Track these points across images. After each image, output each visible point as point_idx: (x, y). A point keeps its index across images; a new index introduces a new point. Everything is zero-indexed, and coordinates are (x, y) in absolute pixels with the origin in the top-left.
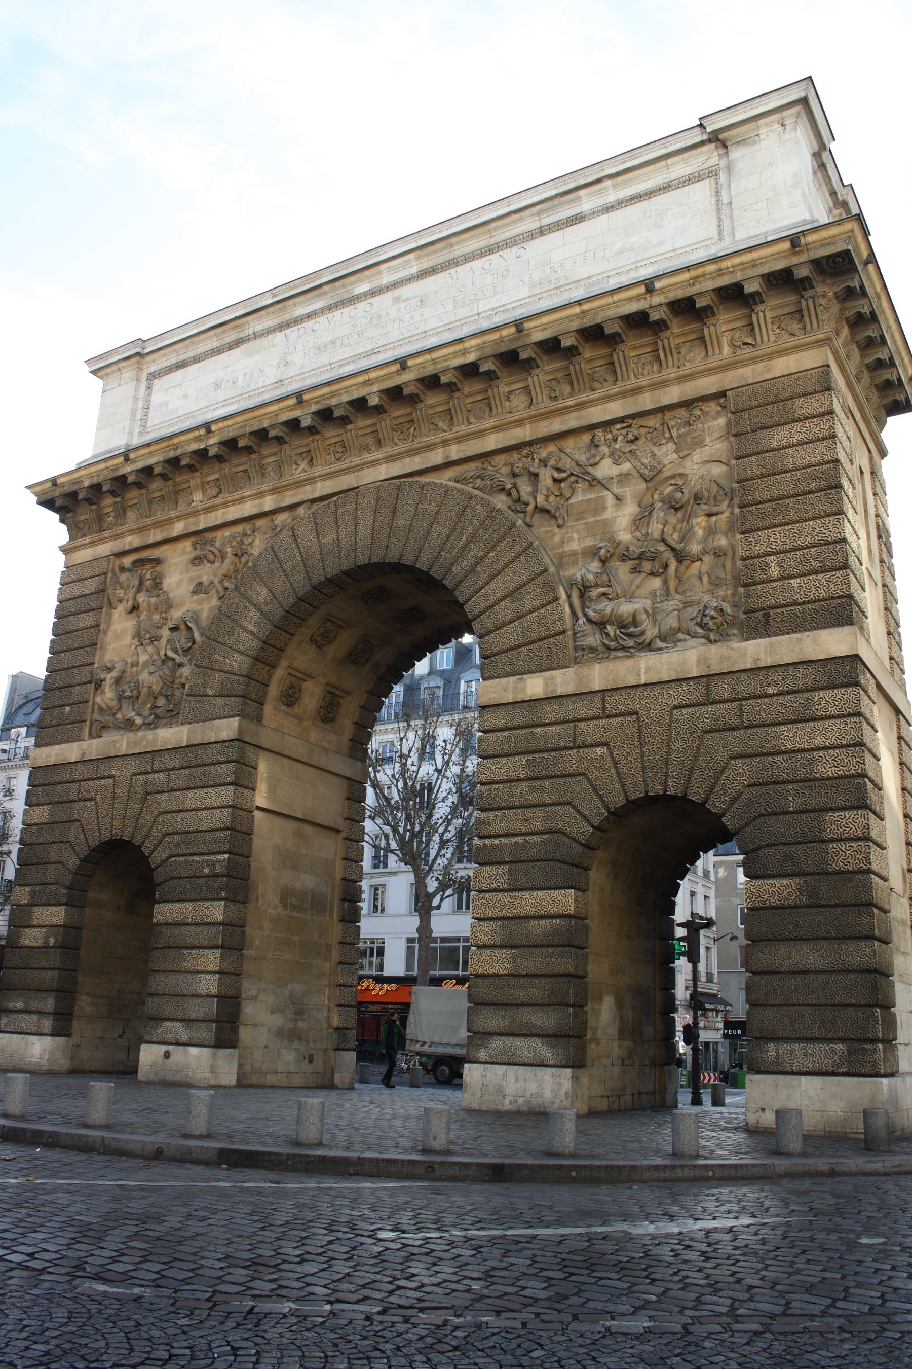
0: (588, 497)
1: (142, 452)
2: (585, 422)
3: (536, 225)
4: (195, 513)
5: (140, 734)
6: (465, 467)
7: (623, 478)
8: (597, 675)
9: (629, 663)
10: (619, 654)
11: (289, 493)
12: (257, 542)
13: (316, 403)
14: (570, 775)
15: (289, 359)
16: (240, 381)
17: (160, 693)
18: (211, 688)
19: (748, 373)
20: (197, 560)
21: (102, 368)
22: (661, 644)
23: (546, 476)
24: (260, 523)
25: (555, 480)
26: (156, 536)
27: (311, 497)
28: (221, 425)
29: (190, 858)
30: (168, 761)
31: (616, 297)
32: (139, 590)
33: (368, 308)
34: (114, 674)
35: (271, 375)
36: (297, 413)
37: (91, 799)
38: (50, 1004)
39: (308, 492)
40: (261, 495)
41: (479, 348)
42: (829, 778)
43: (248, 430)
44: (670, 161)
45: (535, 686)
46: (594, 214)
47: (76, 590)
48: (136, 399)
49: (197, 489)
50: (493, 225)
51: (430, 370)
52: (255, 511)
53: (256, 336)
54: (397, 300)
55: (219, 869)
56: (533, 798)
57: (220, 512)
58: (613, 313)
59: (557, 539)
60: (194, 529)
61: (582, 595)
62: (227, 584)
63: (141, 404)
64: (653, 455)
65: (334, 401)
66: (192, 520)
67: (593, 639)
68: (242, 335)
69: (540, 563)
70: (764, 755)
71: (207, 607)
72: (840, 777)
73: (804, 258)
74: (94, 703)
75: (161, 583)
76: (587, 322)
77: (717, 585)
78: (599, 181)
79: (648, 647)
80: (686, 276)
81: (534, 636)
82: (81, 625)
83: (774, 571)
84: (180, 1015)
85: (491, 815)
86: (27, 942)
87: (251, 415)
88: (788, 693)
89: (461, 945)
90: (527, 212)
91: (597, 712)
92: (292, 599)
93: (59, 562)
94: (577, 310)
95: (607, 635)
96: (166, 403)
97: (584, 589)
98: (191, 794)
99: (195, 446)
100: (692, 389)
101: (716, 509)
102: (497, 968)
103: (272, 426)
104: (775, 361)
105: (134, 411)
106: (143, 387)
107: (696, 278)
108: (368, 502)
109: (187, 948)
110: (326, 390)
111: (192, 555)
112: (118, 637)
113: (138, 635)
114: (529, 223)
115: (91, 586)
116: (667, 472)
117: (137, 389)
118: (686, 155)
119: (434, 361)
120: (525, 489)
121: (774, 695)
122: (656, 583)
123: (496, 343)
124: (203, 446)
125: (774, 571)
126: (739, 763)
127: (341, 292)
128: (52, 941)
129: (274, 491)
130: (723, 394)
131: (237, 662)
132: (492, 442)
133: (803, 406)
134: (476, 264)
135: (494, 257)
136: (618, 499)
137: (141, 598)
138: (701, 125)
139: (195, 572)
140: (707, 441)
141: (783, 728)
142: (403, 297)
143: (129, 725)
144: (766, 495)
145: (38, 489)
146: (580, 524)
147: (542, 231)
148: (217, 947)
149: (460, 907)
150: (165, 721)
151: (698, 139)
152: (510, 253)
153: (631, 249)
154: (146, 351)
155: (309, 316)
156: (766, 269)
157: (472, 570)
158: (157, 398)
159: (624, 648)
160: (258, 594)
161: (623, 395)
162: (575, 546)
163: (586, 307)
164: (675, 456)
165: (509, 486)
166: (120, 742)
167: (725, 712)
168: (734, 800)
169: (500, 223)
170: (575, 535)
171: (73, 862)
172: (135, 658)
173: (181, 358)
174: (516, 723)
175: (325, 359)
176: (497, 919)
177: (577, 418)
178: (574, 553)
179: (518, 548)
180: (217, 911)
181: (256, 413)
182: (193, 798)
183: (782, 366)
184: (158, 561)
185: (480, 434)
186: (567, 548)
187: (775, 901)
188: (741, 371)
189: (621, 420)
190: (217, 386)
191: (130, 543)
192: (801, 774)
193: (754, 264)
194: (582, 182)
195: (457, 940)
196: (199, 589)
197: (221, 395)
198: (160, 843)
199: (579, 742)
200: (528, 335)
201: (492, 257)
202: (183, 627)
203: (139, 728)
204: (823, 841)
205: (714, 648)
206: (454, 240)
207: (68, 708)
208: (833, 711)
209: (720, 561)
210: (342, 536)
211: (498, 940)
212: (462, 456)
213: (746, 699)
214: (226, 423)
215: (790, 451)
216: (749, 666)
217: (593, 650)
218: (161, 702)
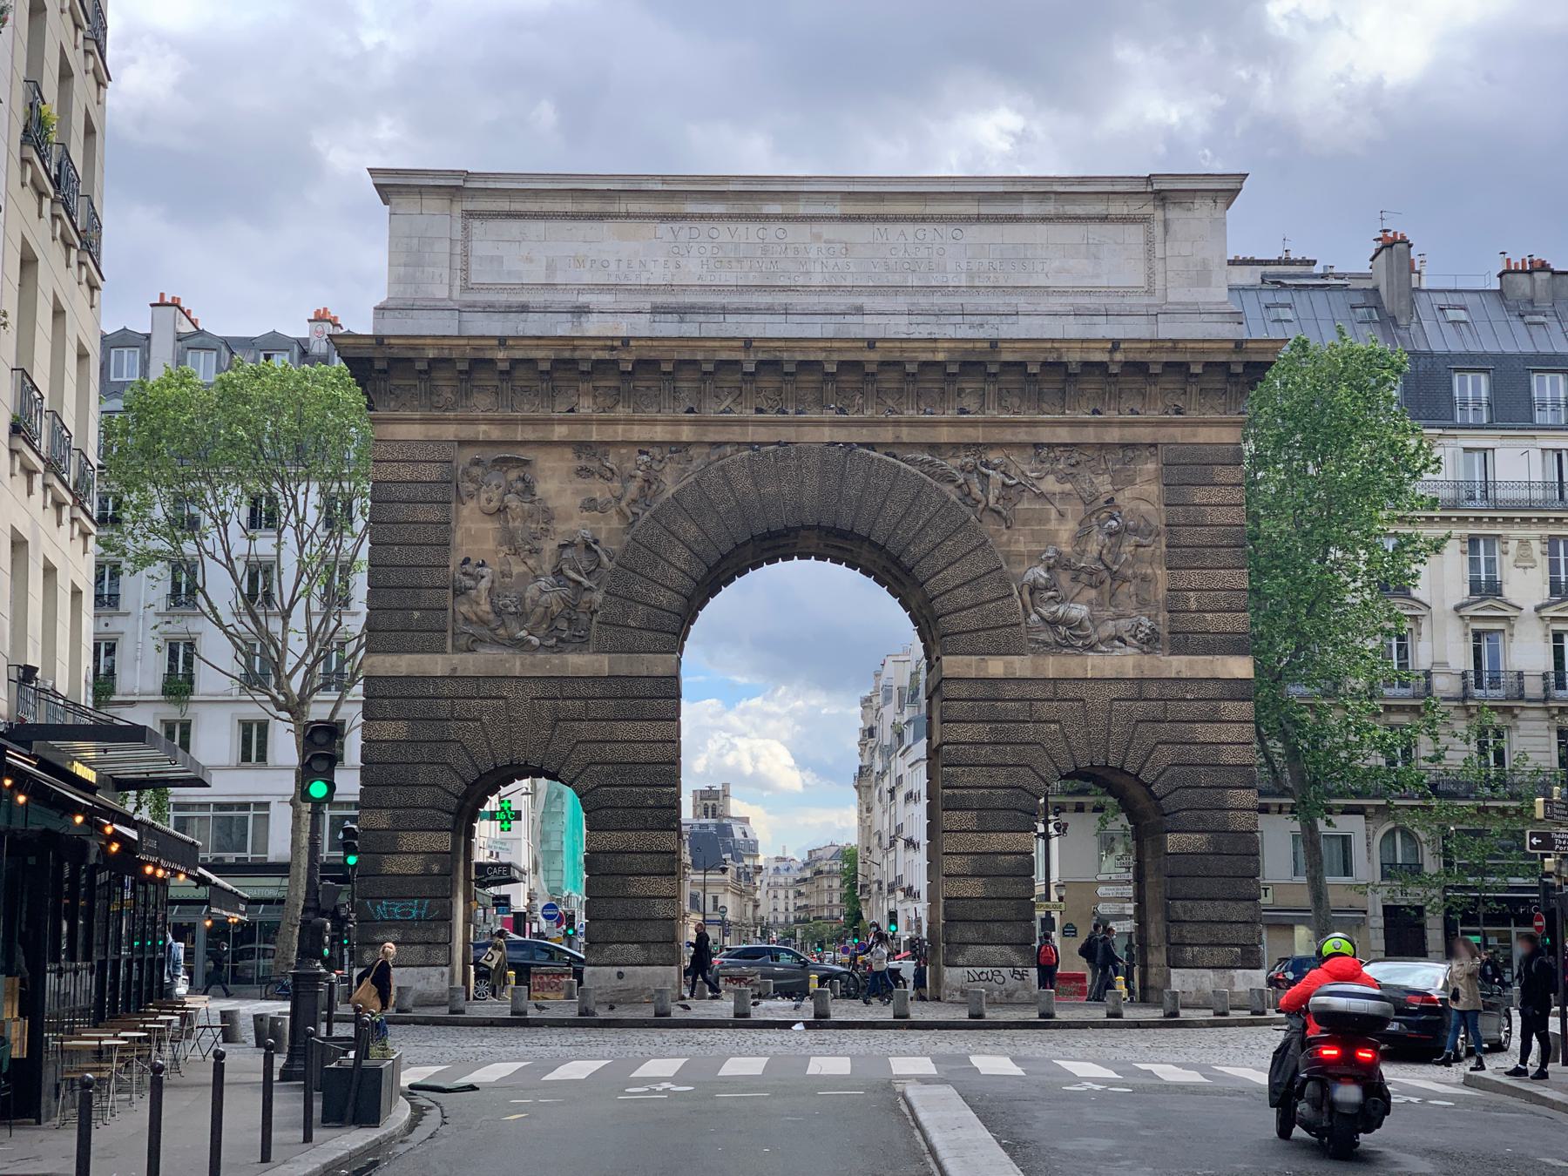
4: (586, 421)
5: (540, 656)
7: (1065, 496)
8: (1052, 666)
9: (1078, 660)
12: (667, 469)
16: (613, 267)
17: (560, 615)
19: (1179, 434)
20: (584, 472)
25: (1004, 484)
26: (529, 434)
27: (741, 440)
30: (583, 690)
36: (740, 356)
39: (735, 434)
40: (677, 422)
41: (949, 350)
45: (996, 667)
46: (1033, 219)
49: (586, 394)
51: (896, 356)
52: (668, 438)
53: (628, 216)
54: (818, 237)
56: (996, 759)
57: (620, 428)
59: (1005, 538)
61: (1031, 594)
62: (635, 510)
63: (458, 249)
65: (785, 356)
69: (996, 559)
77: (1145, 605)
79: (1091, 648)
81: (992, 624)
85: (959, 770)
89: (251, 813)
91: (1049, 695)
96: (500, 260)
97: (1034, 589)
98: (621, 725)
100: (1130, 435)
101: (1145, 542)
103: (707, 361)
106: (458, 225)
111: (578, 464)
114: (971, 209)
119: (902, 350)
120: (976, 490)
122: (1093, 593)
125: (1193, 605)
126: (1165, 747)
130: (1154, 445)
132: (944, 435)
134: (909, 229)
136: (1062, 515)
139: (582, 484)
142: (825, 237)
143: (519, 645)
144: (1188, 542)
147: (979, 219)
149: (246, 757)
150: (571, 647)
152: (947, 230)
154: (468, 185)
162: (1021, 548)
165: (961, 481)
167: (1156, 708)
171: (457, 786)
174: (978, 695)
178: (1021, 554)
179: (975, 542)
182: (624, 730)
183: (1205, 435)
184: (526, 463)
187: (1191, 849)
188: (1171, 430)
189: (1065, 445)
192: (1209, 760)
193: (1203, 351)
195: (245, 806)
196: (590, 505)
199: (1035, 717)
201: (925, 226)
203: (536, 649)
207: (417, 614)
209: (1145, 585)
211: (968, 870)
217: (1046, 644)
218: (564, 625)
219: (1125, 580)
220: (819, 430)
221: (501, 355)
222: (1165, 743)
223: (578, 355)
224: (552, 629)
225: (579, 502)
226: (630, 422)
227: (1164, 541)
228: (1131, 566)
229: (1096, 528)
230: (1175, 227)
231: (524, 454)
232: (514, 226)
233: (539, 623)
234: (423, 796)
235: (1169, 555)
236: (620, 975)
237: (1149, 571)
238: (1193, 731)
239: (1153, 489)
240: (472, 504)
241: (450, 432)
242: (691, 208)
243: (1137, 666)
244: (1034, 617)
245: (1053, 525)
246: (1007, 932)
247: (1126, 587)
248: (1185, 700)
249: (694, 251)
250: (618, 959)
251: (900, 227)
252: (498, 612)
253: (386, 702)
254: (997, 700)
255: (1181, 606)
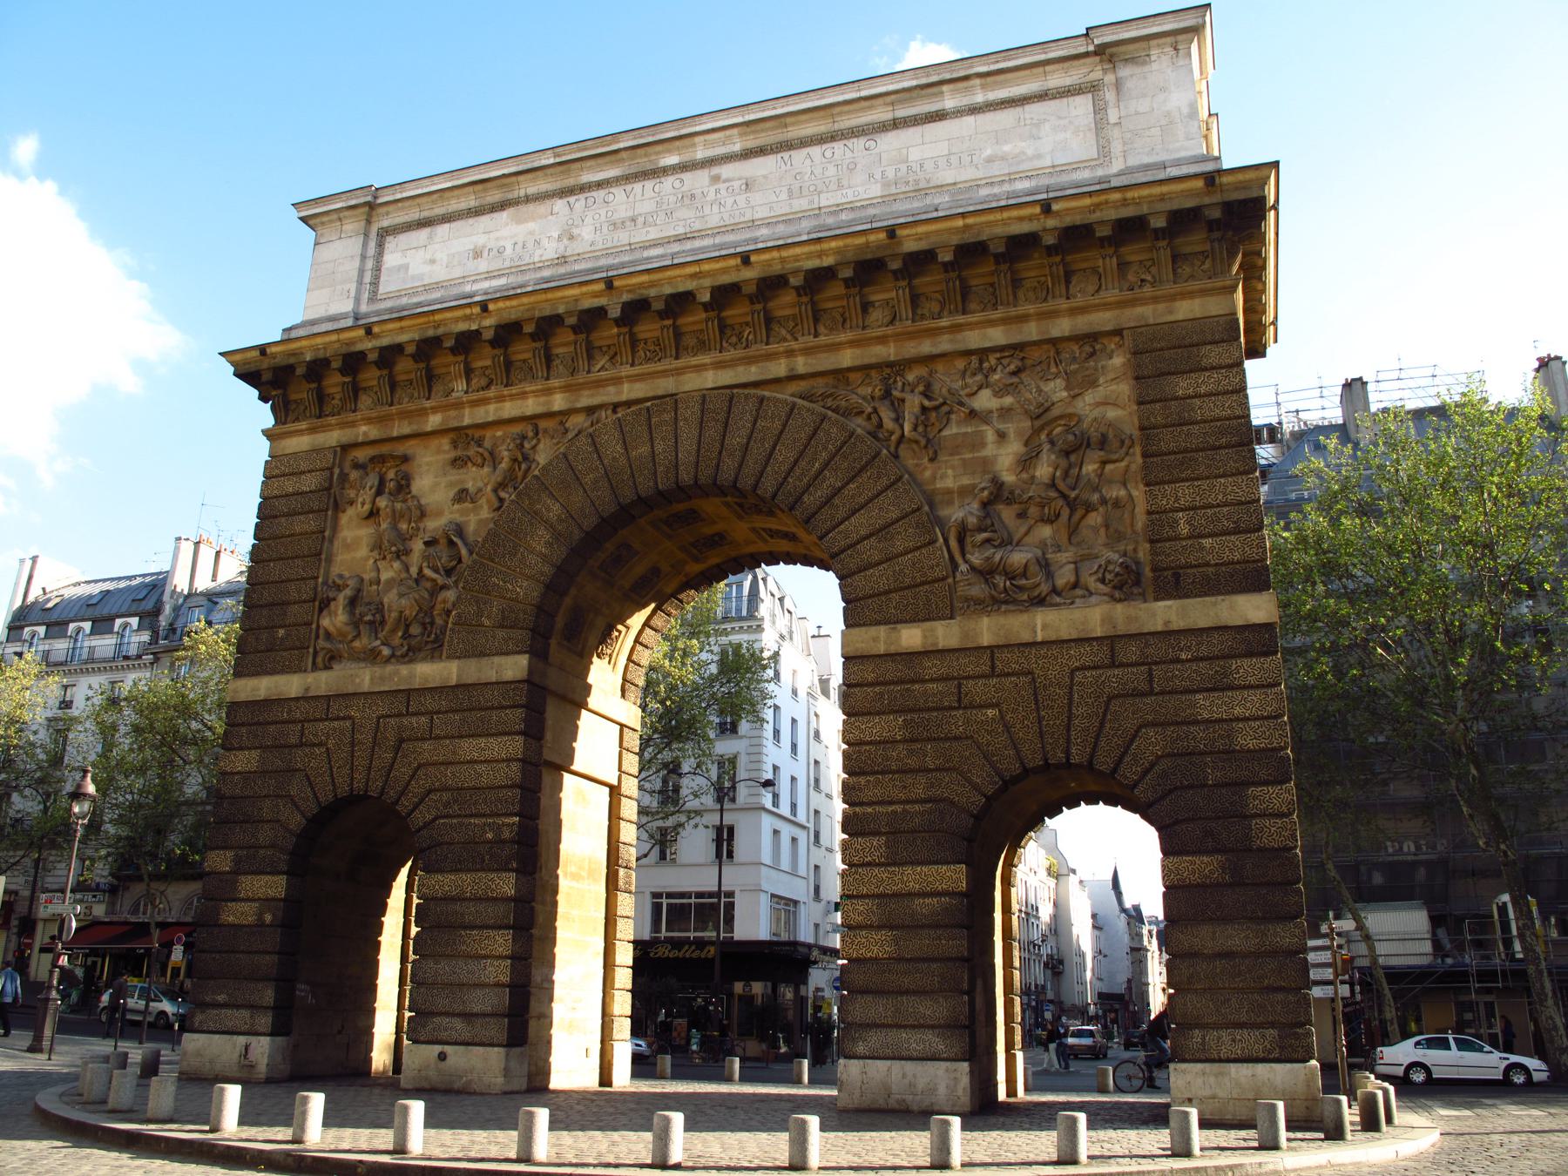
0: (963, 430)
1: (391, 326)
2: (961, 347)
3: (889, 116)
4: (458, 405)
5: (389, 668)
6: (812, 382)
7: (1005, 412)
8: (987, 629)
9: (1024, 617)
10: (1011, 607)
11: (586, 393)
12: (541, 446)
13: (629, 291)
14: (956, 738)
15: (575, 231)
16: (509, 251)
18: (488, 617)
19: (1148, 313)
20: (458, 463)
21: (316, 215)
22: (1058, 600)
23: (913, 402)
24: (543, 424)
25: (924, 409)
26: (406, 429)
28: (501, 304)
29: (466, 821)
30: (430, 703)
31: (1006, 215)
32: (379, 492)
33: (677, 184)
34: (348, 592)
35: (550, 250)
36: (603, 301)
37: (321, 744)
38: (268, 996)
41: (838, 251)
42: (1249, 751)
43: (537, 314)
44: (1048, 68)
45: (911, 637)
46: (959, 113)
47: (289, 486)
48: (363, 257)
50: (838, 110)
52: (540, 410)
53: (528, 199)
55: (506, 835)
56: (912, 762)
57: (492, 407)
58: (1000, 231)
59: (928, 474)
60: (455, 424)
61: (961, 541)
63: (370, 264)
64: (1040, 391)
65: (653, 292)
66: (453, 413)
67: (978, 590)
68: (510, 196)
70: (1177, 723)
71: (478, 519)
72: (1263, 750)
73: (1217, 198)
74: (318, 627)
75: (408, 486)
76: (969, 238)
78: (966, 78)
79: (1040, 601)
80: (1087, 201)
82: (298, 529)
83: (1184, 529)
84: (458, 1008)
85: (862, 780)
86: (231, 919)
87: (542, 297)
88: (1202, 659)
90: (880, 101)
92: (594, 520)
93: (262, 450)
94: (960, 223)
95: (995, 586)
96: (406, 267)
99: (462, 327)
100: (1084, 323)
101: (1114, 457)
102: (875, 951)
104: (1178, 304)
105: (361, 272)
106: (372, 244)
107: (1098, 205)
108: (690, 412)
109: (465, 928)
110: (645, 278)
111: (453, 455)
112: (348, 547)
113: (377, 546)
114: (881, 114)
115: (310, 482)
116: (1055, 412)
117: (365, 245)
118: (1066, 65)
119: (783, 260)
121: (1188, 661)
123: (859, 248)
124: (474, 327)
125: (1184, 529)
127: (643, 162)
128: (268, 918)
129: (567, 388)
130: (1118, 332)
131: (525, 590)
132: (847, 358)
133: (1213, 355)
134: (815, 151)
135: (838, 146)
136: (1002, 436)
137: (382, 502)
138: (1087, 35)
139: (454, 475)
140: (1101, 380)
141: (1198, 696)
142: (724, 176)
143: (372, 656)
145: (237, 357)
146: (956, 460)
147: (896, 124)
148: (507, 927)
151: (1082, 50)
152: (858, 143)
153: (1003, 159)
154: (380, 201)
155: (600, 185)
156: (1175, 206)
157: (828, 500)
158: (391, 259)
159: (1015, 602)
160: (548, 510)
161: (1005, 321)
162: (949, 483)
163: (970, 221)
164: (1065, 394)
166: (364, 678)
168: (1147, 772)
169: (846, 108)
170: (950, 472)
171: (296, 821)
172: (374, 574)
173: (426, 214)
174: (888, 677)
175: (623, 237)
176: (873, 896)
177: (951, 341)
178: (949, 492)
180: (506, 884)
181: (550, 296)
182: (469, 748)
184: (405, 459)
185: (834, 347)
186: (939, 485)
187: (1195, 879)
188: (1139, 310)
190: (477, 254)
191: (365, 434)
192: (1220, 745)
193: (1162, 198)
194: (948, 76)
196: (462, 496)
197: (483, 266)
198: (422, 801)
200: (900, 243)
201: (834, 144)
202: (443, 541)
203: (388, 660)
204: (1245, 817)
205: (1119, 607)
206: (789, 120)
207: (281, 632)
208: (1252, 680)
210: (659, 448)
212: (810, 370)
213: (1156, 663)
214: (508, 303)
215: (1197, 402)
216: (1160, 628)
217: (979, 602)
218: (415, 630)
219: (1089, 508)
220: (705, 376)
221: (370, 345)
222: (1153, 724)
223: (440, 331)
224: (407, 636)
225: (451, 494)
226: (500, 399)
227: (1138, 450)
228: (1096, 489)
229: (1046, 447)
230: (1129, 84)
231: (400, 449)
232: (423, 234)
233: (394, 631)
234: (265, 834)
235: (1145, 467)
236: (442, 1057)
237: (1123, 493)
238: (1193, 705)
239: (1124, 389)
240: (351, 512)
241: (333, 437)
242: (587, 177)
243: (1108, 620)
244: (963, 567)
245: (989, 451)
246: (930, 1009)
247: (1095, 519)
248: (1178, 660)
249: (588, 220)
250: (444, 1035)
251: (805, 151)
252: (356, 623)
253: (244, 730)
254: (913, 681)
255: (1167, 532)
